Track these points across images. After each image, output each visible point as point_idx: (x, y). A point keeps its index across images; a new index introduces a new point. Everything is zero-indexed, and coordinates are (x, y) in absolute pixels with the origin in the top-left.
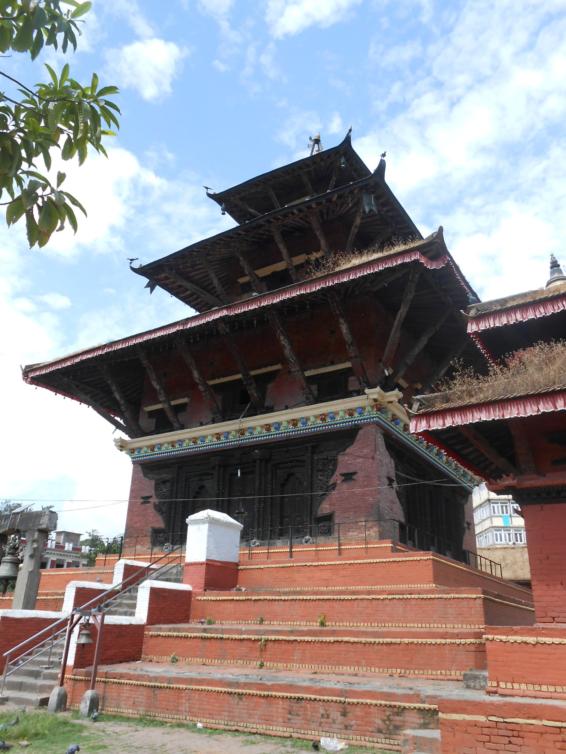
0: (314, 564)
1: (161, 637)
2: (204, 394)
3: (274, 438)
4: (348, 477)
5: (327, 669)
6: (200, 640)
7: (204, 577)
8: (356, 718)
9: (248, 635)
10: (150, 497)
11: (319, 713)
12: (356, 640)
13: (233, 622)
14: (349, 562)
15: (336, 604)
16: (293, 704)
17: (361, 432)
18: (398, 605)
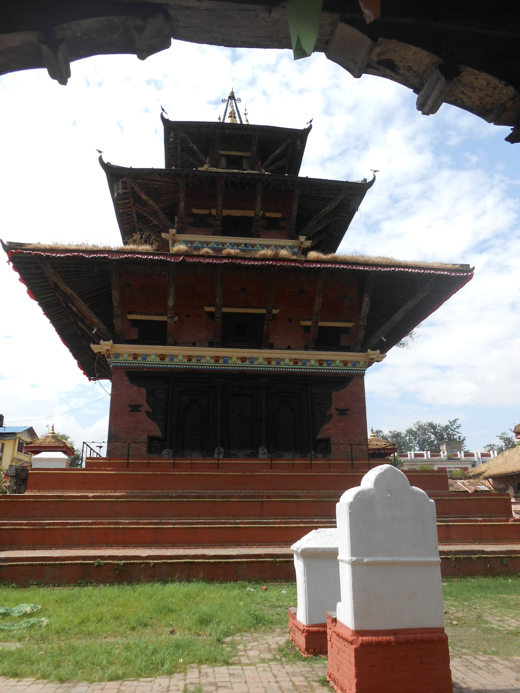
10: (141, 406)
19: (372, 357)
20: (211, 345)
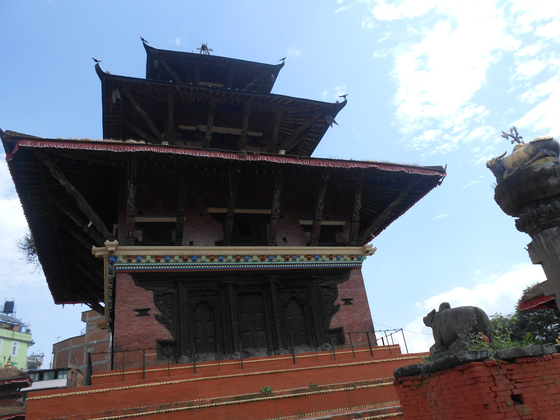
4: (348, 301)
10: (149, 309)
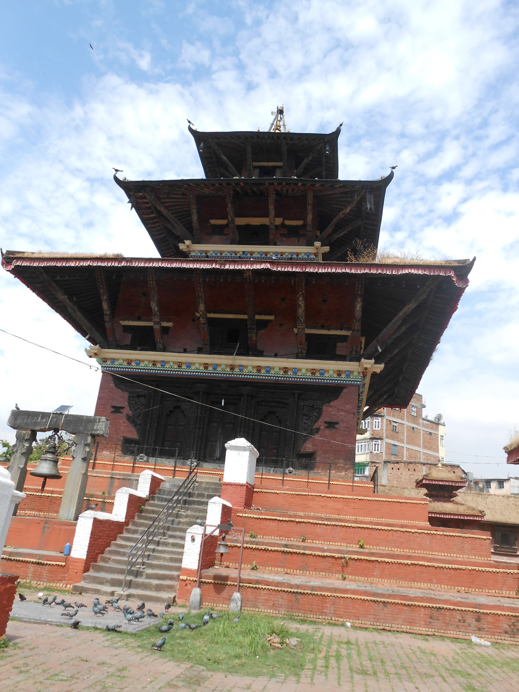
0: (328, 495)
1: (237, 548)
2: (202, 326)
3: (263, 379)
4: (331, 425)
5: (403, 584)
6: (280, 553)
7: (244, 497)
8: (488, 623)
9: (331, 553)
10: (123, 408)
11: (456, 618)
12: (430, 564)
13: (276, 538)
14: (360, 498)
15: (373, 532)
16: (434, 612)
17: (345, 391)
18: (426, 538)
19: (365, 366)
20: (200, 351)
